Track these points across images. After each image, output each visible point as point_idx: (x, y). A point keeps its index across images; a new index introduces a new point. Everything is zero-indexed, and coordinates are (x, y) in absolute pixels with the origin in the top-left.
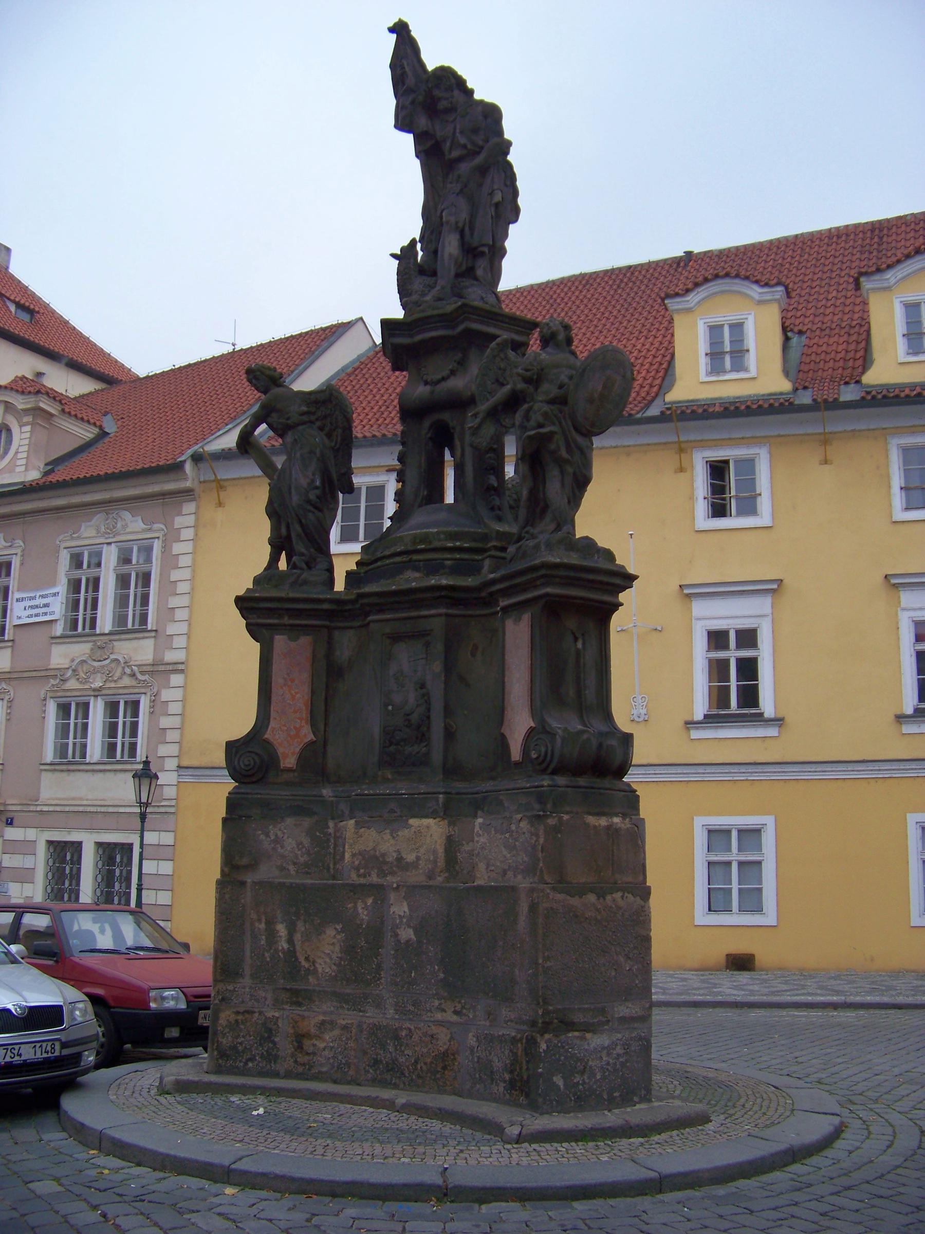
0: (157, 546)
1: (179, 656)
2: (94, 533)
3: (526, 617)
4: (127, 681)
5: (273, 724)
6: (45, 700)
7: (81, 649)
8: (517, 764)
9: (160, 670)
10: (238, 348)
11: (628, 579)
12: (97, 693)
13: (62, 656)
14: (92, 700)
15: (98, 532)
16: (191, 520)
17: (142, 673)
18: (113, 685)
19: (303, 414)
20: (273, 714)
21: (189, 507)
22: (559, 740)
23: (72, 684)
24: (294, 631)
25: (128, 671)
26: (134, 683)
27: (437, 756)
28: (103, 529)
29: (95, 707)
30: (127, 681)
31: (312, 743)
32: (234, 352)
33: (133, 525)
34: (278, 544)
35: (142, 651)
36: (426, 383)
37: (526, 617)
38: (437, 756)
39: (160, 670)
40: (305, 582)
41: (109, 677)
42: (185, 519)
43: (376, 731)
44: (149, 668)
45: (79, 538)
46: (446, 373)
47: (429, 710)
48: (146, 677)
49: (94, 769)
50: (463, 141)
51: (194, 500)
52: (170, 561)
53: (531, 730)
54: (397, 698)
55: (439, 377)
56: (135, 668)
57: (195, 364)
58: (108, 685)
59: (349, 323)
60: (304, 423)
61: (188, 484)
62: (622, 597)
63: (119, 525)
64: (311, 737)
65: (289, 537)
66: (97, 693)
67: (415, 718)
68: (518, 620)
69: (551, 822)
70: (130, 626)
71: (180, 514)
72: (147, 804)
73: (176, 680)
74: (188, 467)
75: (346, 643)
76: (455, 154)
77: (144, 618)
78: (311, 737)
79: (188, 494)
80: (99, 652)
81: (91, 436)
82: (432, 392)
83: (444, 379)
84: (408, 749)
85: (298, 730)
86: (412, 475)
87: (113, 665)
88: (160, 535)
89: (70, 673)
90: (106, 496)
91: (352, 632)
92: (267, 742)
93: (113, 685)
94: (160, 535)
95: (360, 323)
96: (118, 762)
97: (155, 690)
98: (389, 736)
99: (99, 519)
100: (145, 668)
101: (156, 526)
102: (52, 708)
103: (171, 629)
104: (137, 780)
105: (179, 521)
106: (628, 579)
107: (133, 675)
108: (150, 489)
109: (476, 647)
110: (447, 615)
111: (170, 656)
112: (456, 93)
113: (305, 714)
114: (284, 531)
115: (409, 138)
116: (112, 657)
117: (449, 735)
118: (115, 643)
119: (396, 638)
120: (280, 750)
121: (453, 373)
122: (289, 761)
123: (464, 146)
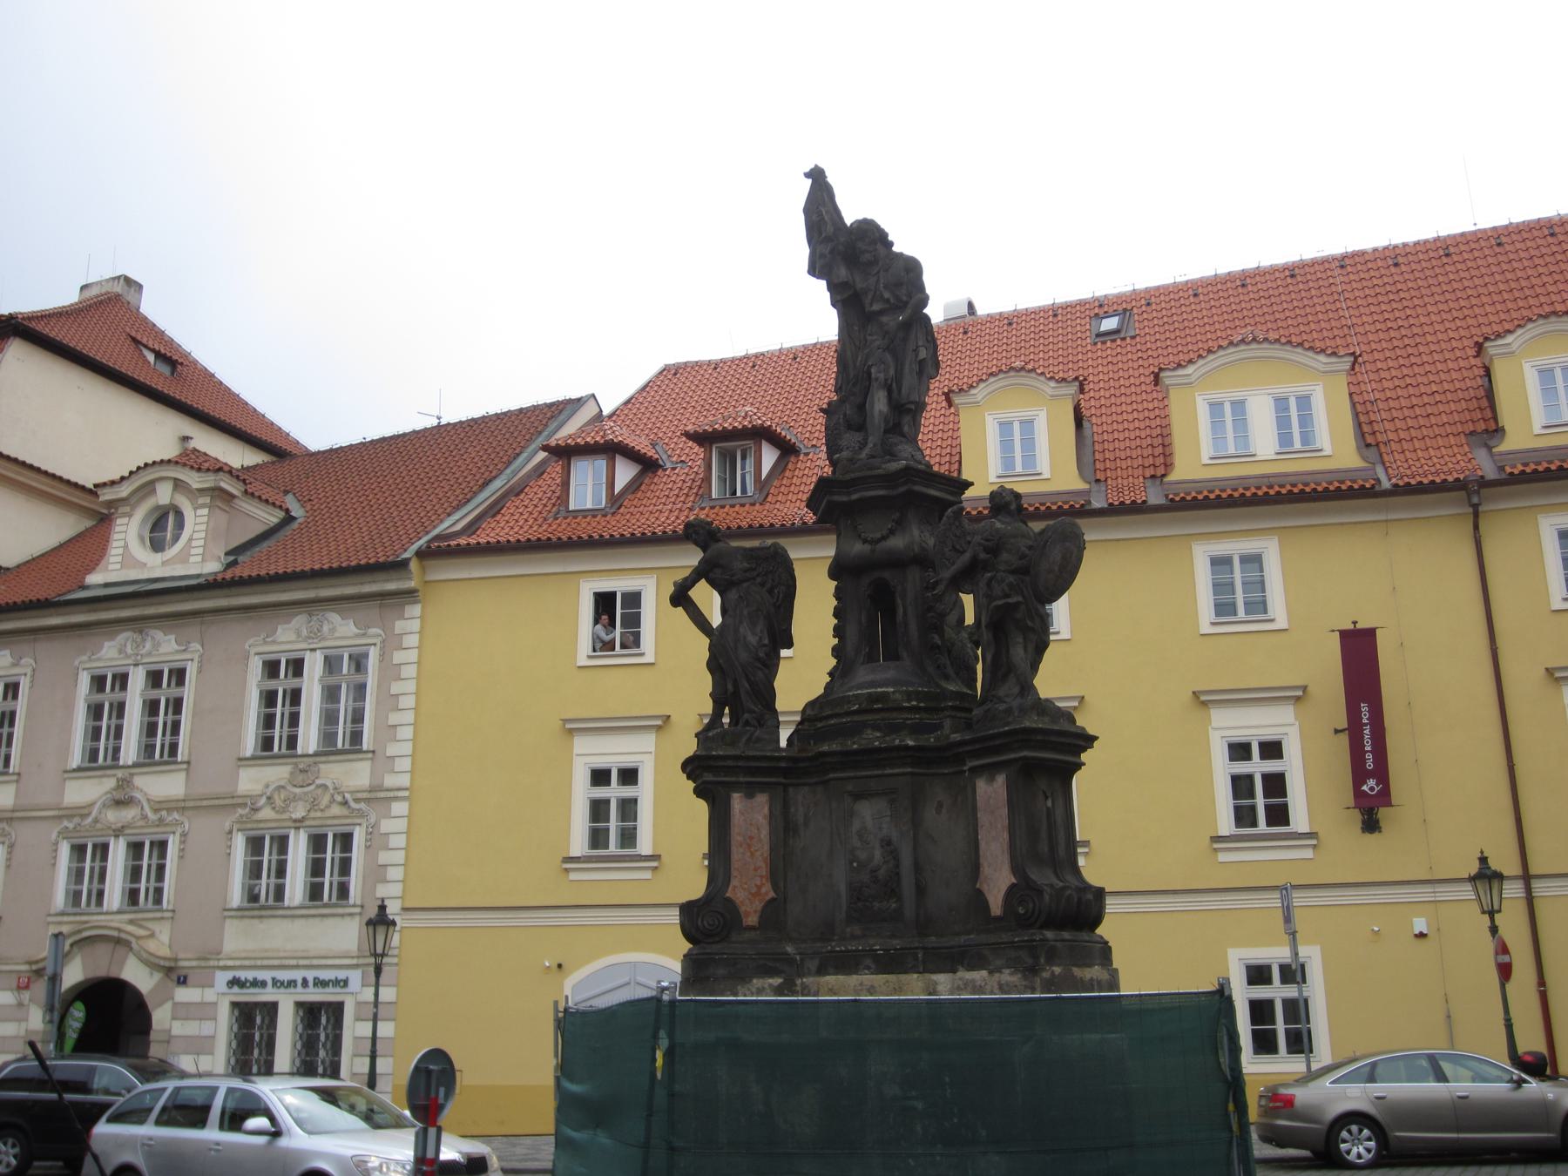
0: (373, 654)
1: (404, 780)
2: (293, 637)
3: (1001, 779)
4: (336, 810)
5: (734, 882)
6: (230, 832)
7: (277, 773)
8: (997, 919)
9: (378, 796)
10: (444, 422)
11: (1088, 740)
12: (298, 824)
13: (251, 781)
14: (292, 833)
15: (298, 633)
16: (415, 625)
17: (357, 800)
18: (319, 814)
19: (746, 571)
20: (734, 873)
21: (415, 610)
22: (1047, 897)
23: (266, 813)
24: (750, 791)
25: (339, 798)
26: (345, 812)
27: (909, 911)
28: (305, 632)
29: (297, 840)
31: (773, 900)
32: (439, 426)
33: (342, 629)
34: (719, 700)
35: (355, 775)
36: (865, 541)
37: (1001, 779)
38: (909, 911)
39: (378, 796)
40: (759, 740)
41: (314, 805)
42: (410, 623)
43: (843, 888)
44: (365, 795)
45: (274, 642)
46: (885, 532)
47: (897, 866)
48: (362, 805)
49: (293, 914)
50: (887, 295)
51: (416, 602)
52: (391, 672)
53: (1013, 886)
54: (863, 856)
55: (878, 535)
56: (348, 796)
57: (391, 438)
58: (312, 814)
59: (579, 400)
60: (748, 580)
61: (412, 584)
62: (1084, 757)
63: (326, 628)
64: (772, 894)
65: (736, 693)
66: (298, 824)
67: (882, 873)
68: (991, 779)
69: (1046, 975)
70: (340, 745)
72: (383, 955)
74: (414, 565)
75: (802, 799)
76: (876, 307)
77: (356, 737)
78: (772, 894)
79: (410, 595)
80: (300, 778)
81: (276, 520)
82: (873, 551)
83: (884, 538)
84: (876, 905)
85: (759, 888)
86: (852, 632)
87: (319, 791)
88: (377, 641)
89: (263, 800)
90: (310, 594)
91: (806, 789)
92: (729, 900)
93: (319, 814)
95: (592, 401)
96: (326, 906)
97: (373, 820)
98: (856, 893)
99: (299, 621)
100: (359, 795)
101: (373, 631)
102: (239, 843)
103: (392, 750)
104: (371, 929)
105: (400, 626)
106: (1088, 740)
107: (345, 803)
109: (940, 805)
110: (912, 774)
111: (390, 781)
112: (879, 246)
113: (764, 871)
114: (730, 687)
115: (823, 284)
116: (318, 782)
117: (921, 890)
118: (322, 766)
119: (858, 796)
120: (742, 909)
121: (892, 532)
122: (752, 920)
123: (888, 301)
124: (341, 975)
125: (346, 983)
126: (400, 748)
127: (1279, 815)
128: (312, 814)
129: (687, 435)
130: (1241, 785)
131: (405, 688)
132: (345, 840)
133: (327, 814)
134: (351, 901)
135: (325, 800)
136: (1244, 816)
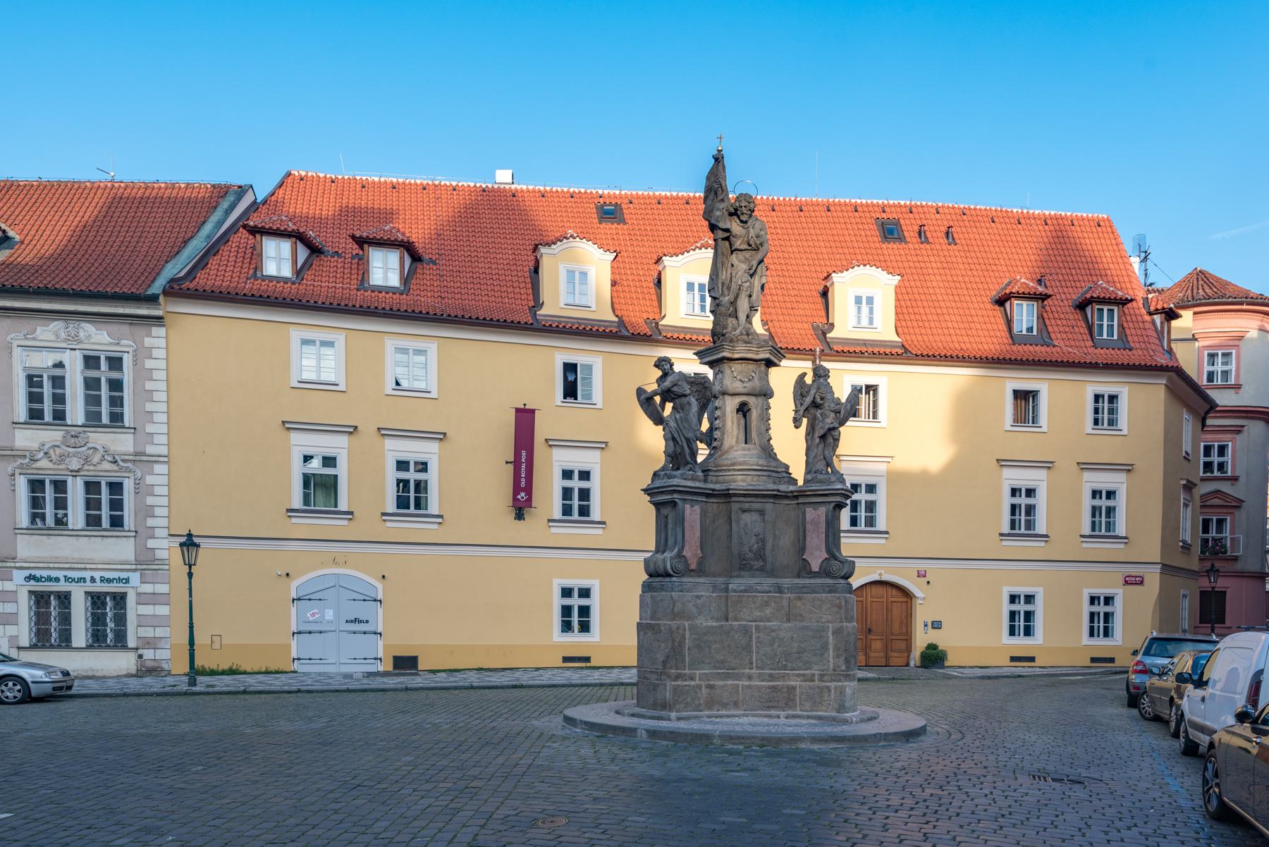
1: (164, 451)
2: (53, 337)
4: (106, 466)
6: (13, 475)
7: (53, 436)
9: (139, 458)
12: (75, 473)
13: (27, 439)
14: (70, 480)
15: (57, 336)
23: (44, 463)
26: (114, 467)
28: (63, 335)
29: (74, 485)
30: (106, 466)
33: (98, 337)
35: (122, 443)
41: (87, 460)
42: (156, 338)
45: (34, 339)
48: (129, 464)
49: (76, 534)
63: (82, 334)
66: (75, 473)
71: (149, 335)
73: (159, 468)
74: (161, 298)
80: (73, 440)
88: (130, 350)
89: (41, 454)
94: (130, 350)
97: (139, 475)
99: (57, 325)
102: (22, 484)
103: (150, 428)
104: (185, 549)
105: (148, 342)
108: (120, 310)
111: (150, 450)
116: (89, 445)
124: (124, 575)
125: (127, 581)
126: (158, 427)
127: (584, 511)
128: (86, 467)
129: (353, 237)
130: (567, 493)
131: (157, 385)
132: (116, 488)
133: (99, 467)
134: (126, 528)
135: (96, 459)
136: (567, 510)
